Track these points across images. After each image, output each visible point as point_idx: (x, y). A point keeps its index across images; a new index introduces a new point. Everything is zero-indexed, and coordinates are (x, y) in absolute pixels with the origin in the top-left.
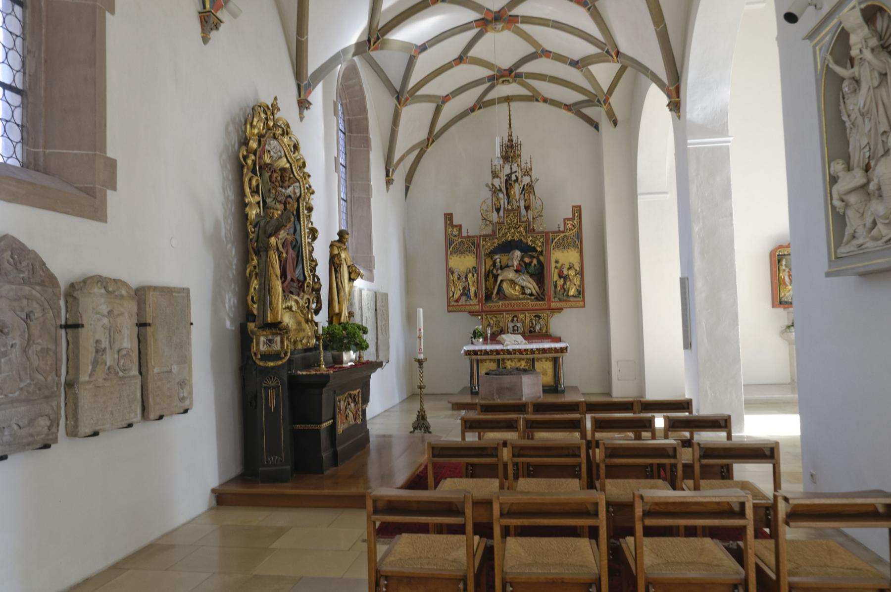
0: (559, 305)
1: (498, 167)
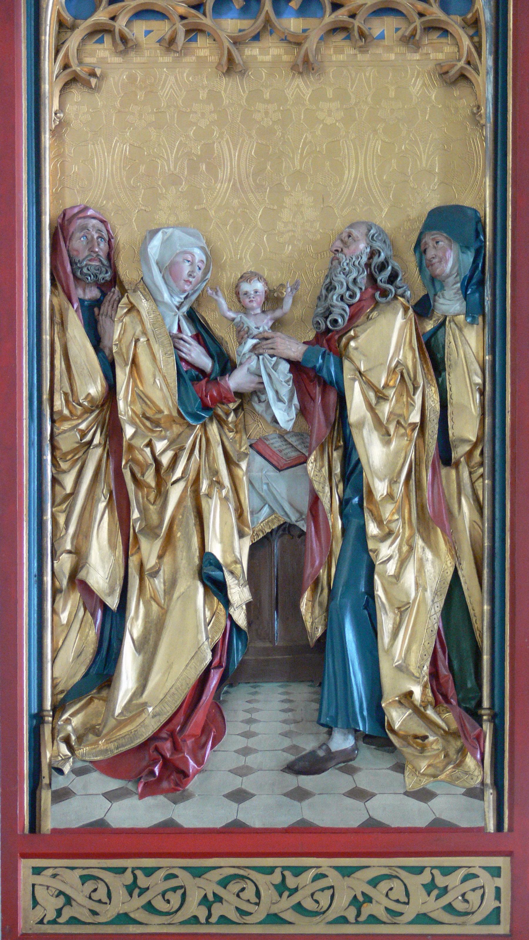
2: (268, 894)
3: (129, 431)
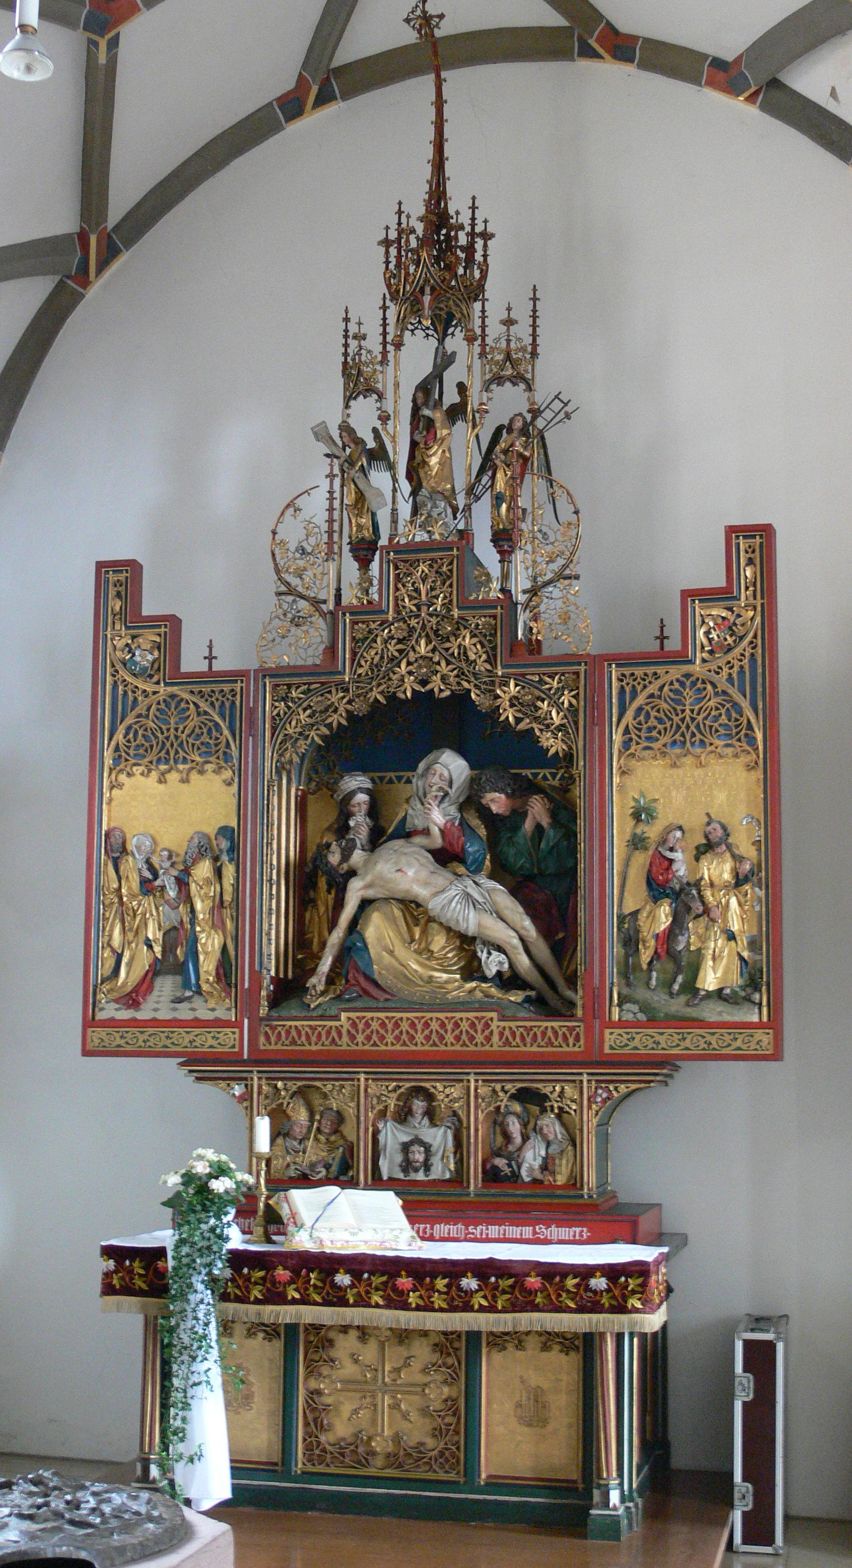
0: (643, 1042)
1: (373, 343)
2: (163, 1038)
3: (125, 899)
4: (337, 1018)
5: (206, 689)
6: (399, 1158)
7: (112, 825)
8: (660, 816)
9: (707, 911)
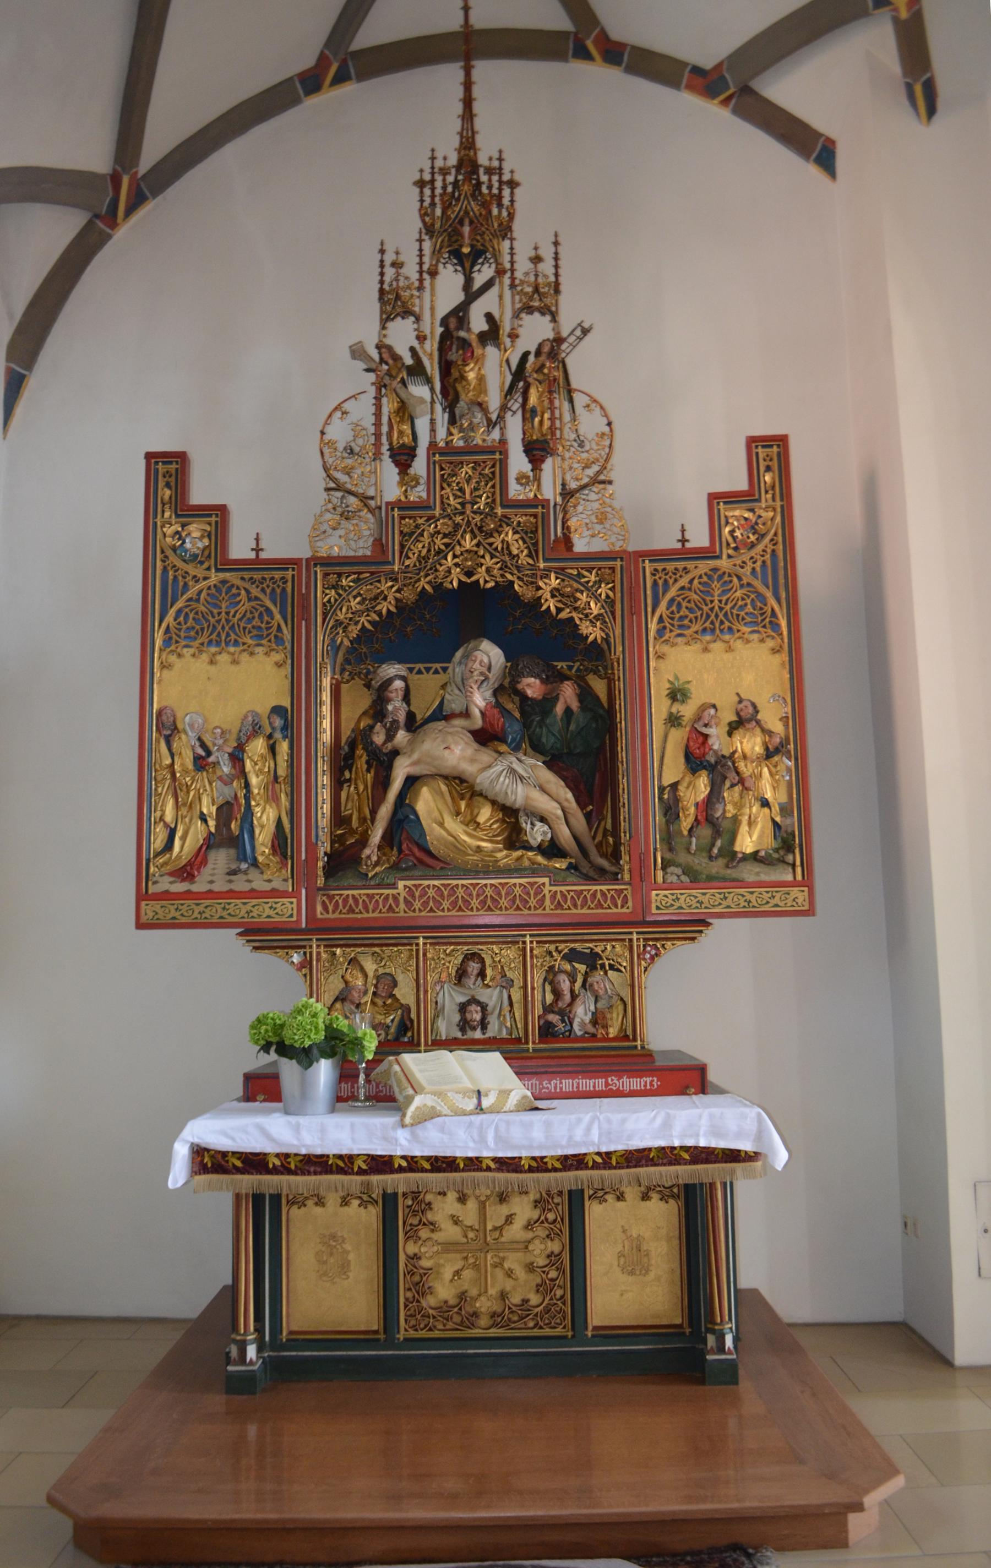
0: (689, 901)
1: (411, 270)
2: (219, 910)
3: (178, 775)
4: (394, 886)
5: (257, 576)
6: (457, 1017)
7: (164, 704)
8: (693, 696)
9: (742, 781)
